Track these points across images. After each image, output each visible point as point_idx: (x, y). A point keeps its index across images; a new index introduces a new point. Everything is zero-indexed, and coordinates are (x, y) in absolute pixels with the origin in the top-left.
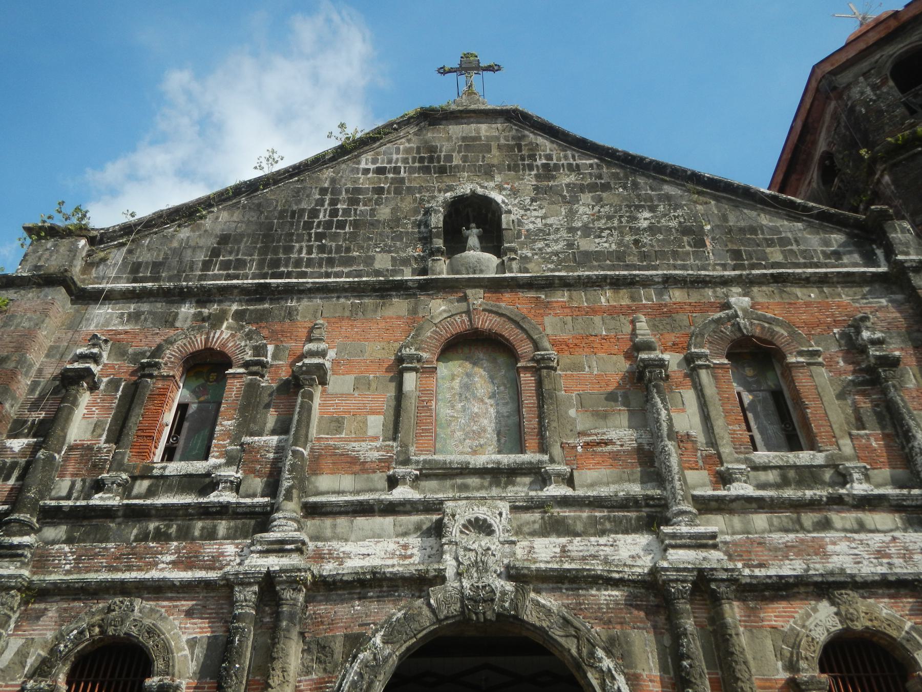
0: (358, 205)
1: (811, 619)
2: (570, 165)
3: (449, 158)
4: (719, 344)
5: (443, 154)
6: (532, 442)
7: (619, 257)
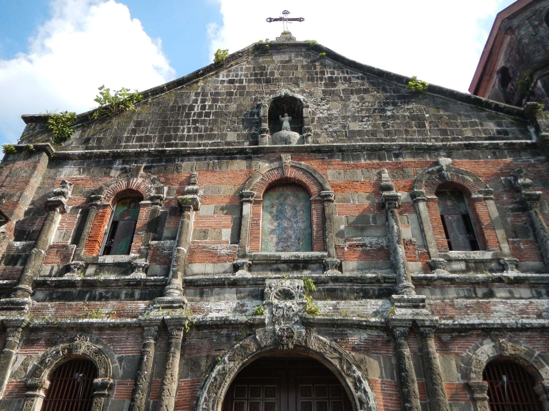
0: (218, 102)
1: (479, 349)
3: (272, 74)
4: (431, 187)
7: (374, 133)
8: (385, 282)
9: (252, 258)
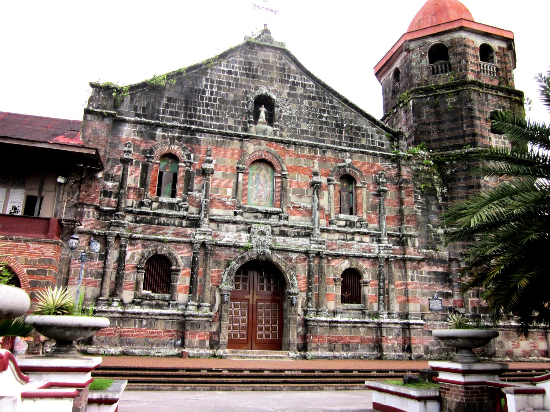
2: (302, 84)
3: (257, 70)
6: (278, 203)
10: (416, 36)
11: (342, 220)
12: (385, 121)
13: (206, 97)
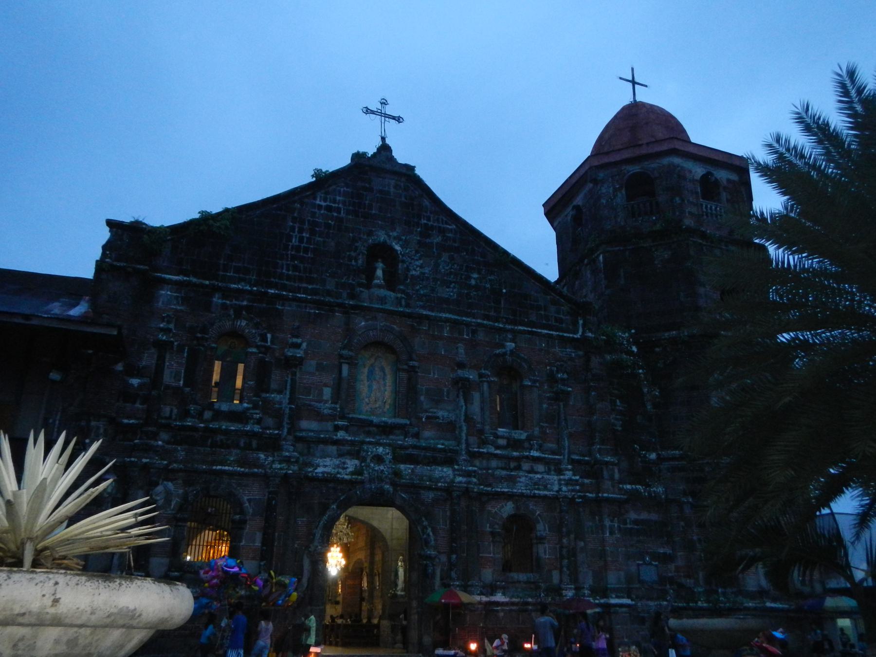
2: (440, 227)
5: (367, 202)
8: (450, 452)
9: (351, 420)
10: (606, 160)
11: (502, 437)
12: (562, 284)
13: (292, 246)
